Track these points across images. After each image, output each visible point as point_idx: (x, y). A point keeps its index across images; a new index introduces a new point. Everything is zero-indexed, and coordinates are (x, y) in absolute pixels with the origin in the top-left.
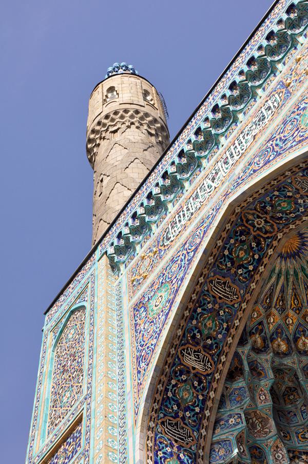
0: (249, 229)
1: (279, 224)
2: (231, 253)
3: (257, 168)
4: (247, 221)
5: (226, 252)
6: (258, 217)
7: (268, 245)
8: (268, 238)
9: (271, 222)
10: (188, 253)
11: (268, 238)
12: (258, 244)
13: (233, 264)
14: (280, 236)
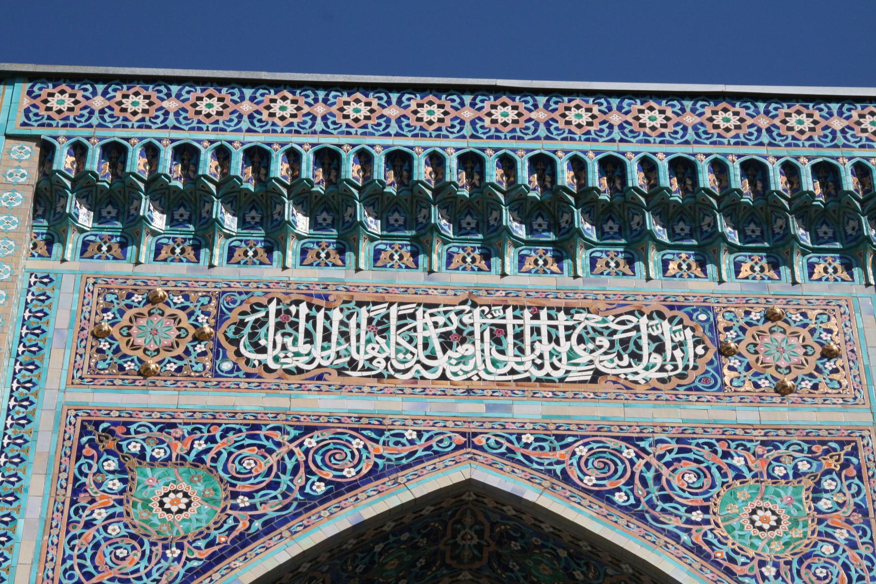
0: (444, 536)
1: (491, 567)
2: (380, 554)
3: (574, 473)
4: (459, 521)
5: (378, 548)
6: (480, 534)
7: (435, 577)
8: (448, 567)
9: (486, 555)
10: (309, 472)
11: (448, 567)
12: (427, 566)
13: (365, 571)
14: (466, 576)
